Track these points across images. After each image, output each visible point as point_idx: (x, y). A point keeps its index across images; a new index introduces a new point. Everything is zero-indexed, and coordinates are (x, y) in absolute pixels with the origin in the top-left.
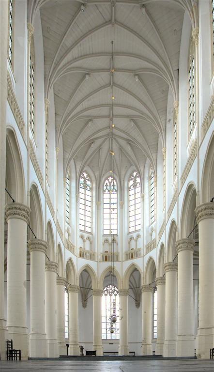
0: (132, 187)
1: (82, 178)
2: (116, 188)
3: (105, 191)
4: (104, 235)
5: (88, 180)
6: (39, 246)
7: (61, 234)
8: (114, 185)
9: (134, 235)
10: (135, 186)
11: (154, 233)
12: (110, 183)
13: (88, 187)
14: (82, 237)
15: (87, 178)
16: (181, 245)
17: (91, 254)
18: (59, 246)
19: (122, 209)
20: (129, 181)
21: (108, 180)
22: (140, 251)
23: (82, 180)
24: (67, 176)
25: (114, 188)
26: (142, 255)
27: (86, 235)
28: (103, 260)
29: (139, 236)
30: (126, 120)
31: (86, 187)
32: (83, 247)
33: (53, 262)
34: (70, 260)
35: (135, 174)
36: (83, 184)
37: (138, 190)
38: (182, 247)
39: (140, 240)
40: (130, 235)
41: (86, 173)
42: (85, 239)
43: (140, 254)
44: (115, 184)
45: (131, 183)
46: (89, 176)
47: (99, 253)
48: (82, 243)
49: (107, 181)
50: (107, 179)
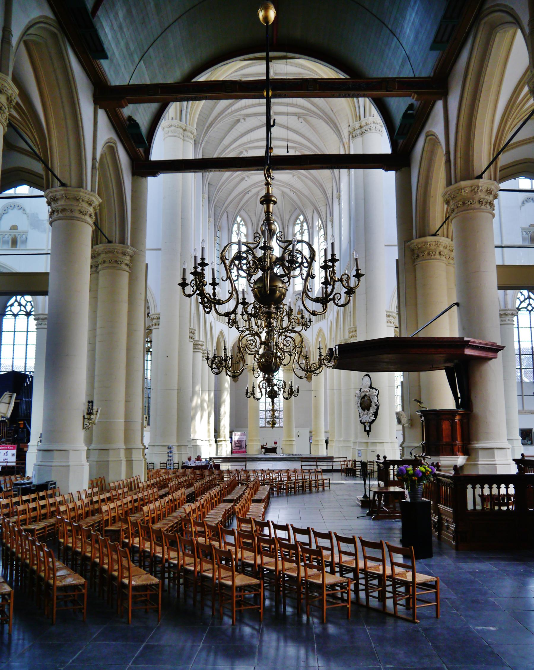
0: (298, 233)
5: (243, 225)
10: (302, 233)
20: (294, 224)
34: (221, 333)
35: (301, 218)
45: (297, 228)
46: (243, 219)
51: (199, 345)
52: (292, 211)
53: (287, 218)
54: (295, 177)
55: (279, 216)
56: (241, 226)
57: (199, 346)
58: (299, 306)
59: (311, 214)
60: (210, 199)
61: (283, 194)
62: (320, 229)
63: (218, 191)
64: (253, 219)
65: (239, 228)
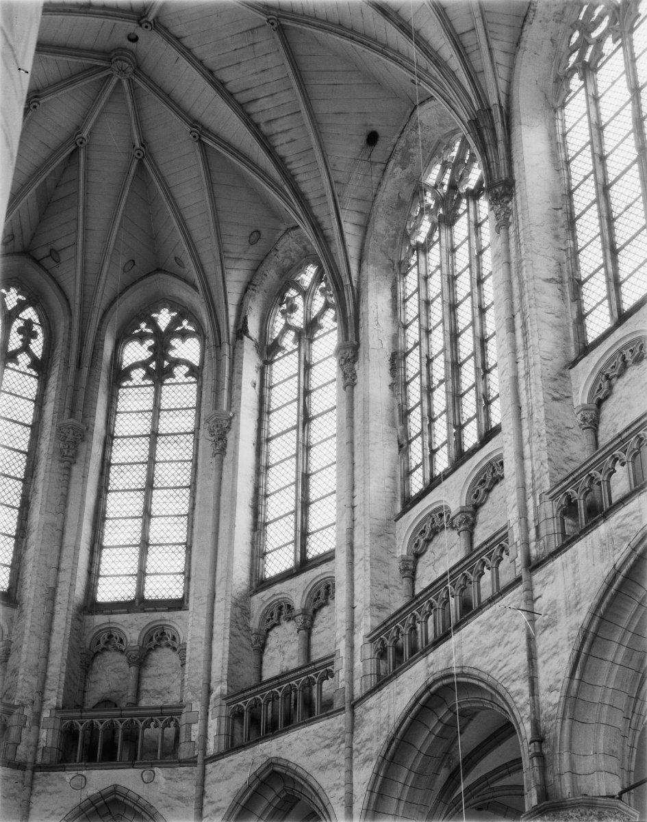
2: (37, 346)
9: (132, 628)
10: (159, 372)
20: (123, 337)
25: (25, 348)
29: (158, 638)
37: (181, 392)
40: (100, 619)
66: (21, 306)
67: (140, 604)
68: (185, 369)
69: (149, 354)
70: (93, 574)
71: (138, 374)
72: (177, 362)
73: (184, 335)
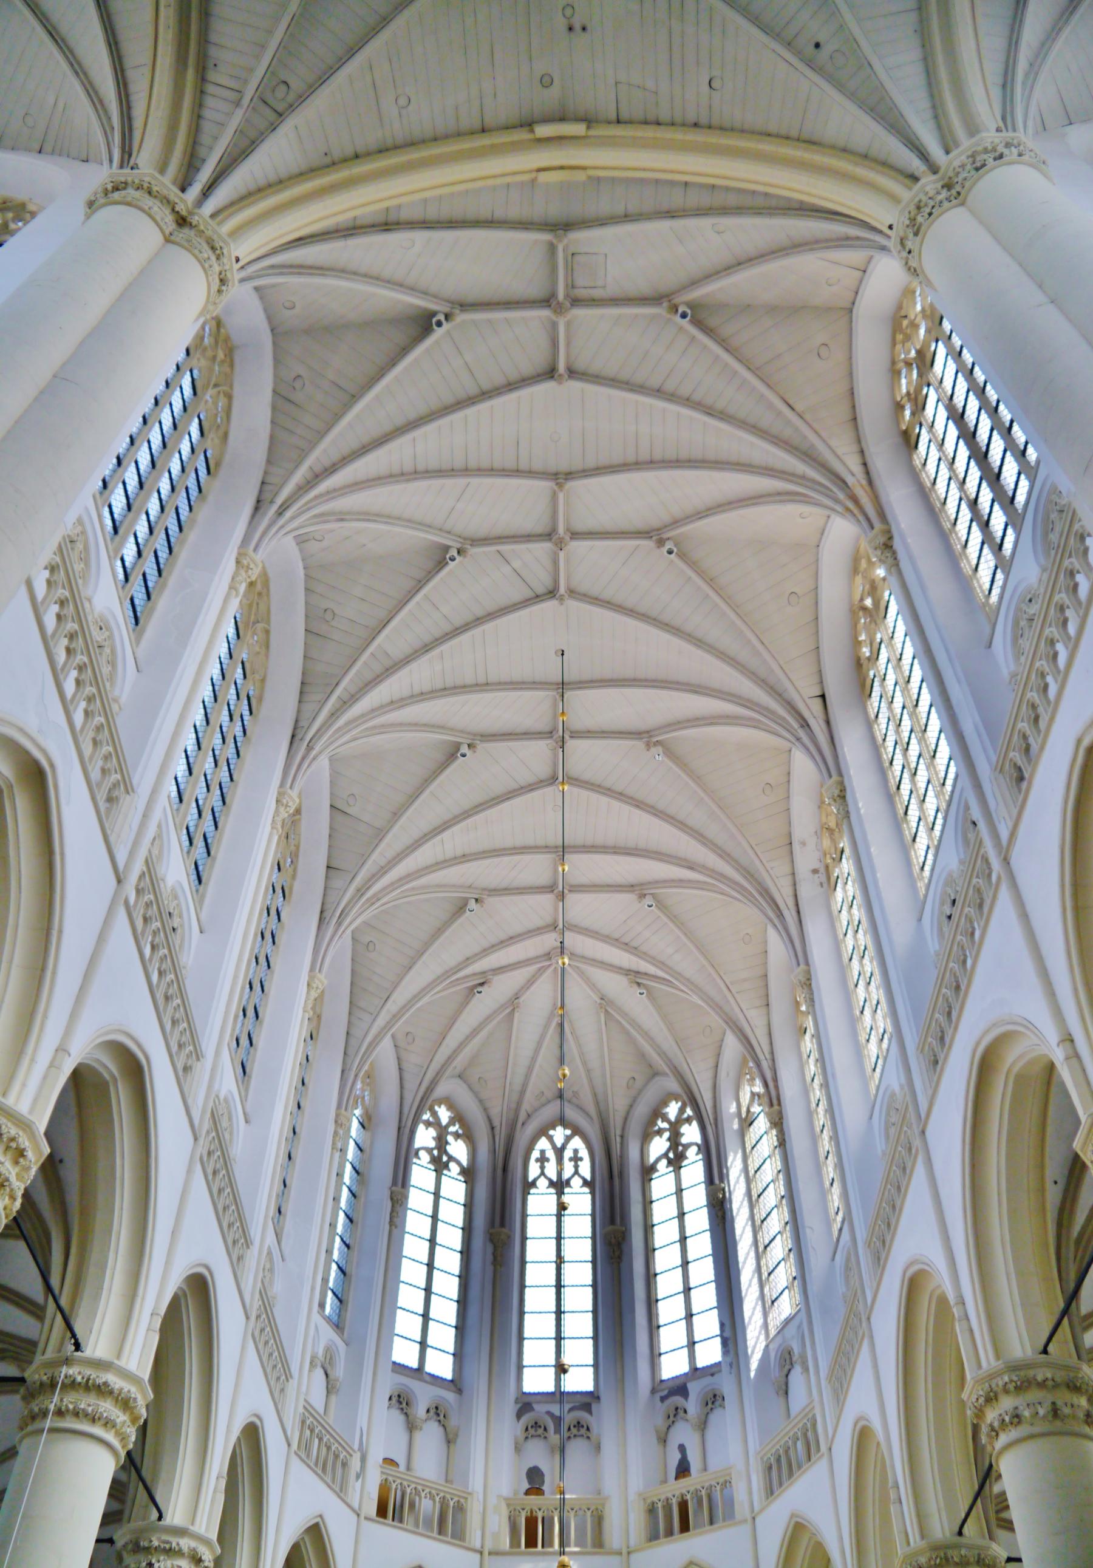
0: (664, 1162)
1: (428, 1124)
3: (533, 1184)
4: (526, 1404)
5: (457, 1136)
6: (86, 1402)
7: (277, 1370)
8: (576, 1159)
10: (676, 1160)
11: (797, 1377)
12: (559, 1152)
13: (452, 1165)
14: (401, 1401)
15: (452, 1129)
16: (1007, 1403)
17: (444, 1503)
18: (252, 1434)
19: (620, 1257)
20: (647, 1136)
21: (550, 1139)
22: (727, 1484)
23: (424, 1137)
24: (357, 1112)
25: (576, 1172)
26: (742, 1508)
27: (423, 1397)
28: (514, 1543)
30: (627, 899)
31: (446, 1166)
32: (402, 1461)
33: (181, 1532)
34: (315, 1532)
35: (672, 1110)
36: (429, 1151)
37: (694, 1170)
38: (1017, 1418)
39: (726, 1420)
41: (451, 1107)
42: (420, 1411)
43: (730, 1503)
44: (584, 1153)
45: (659, 1146)
46: (458, 1117)
47: (492, 1501)
48: (402, 1437)
49: (543, 1144)
50: (543, 1132)
51: (103, 1390)
52: (639, 1083)
53: (618, 1104)
54: (649, 900)
55: (592, 1111)
56: (450, 1138)
57: (107, 1407)
58: (682, 1448)
59: (709, 1074)
60: (327, 914)
61: (606, 1004)
62: (748, 1122)
63: (360, 892)
64: (495, 1112)
65: (441, 1143)
66: (568, 1139)
67: (695, 1371)
68: (694, 1149)
69: (668, 1144)
70: (655, 1355)
71: (662, 1165)
72: (687, 1146)
73: (688, 1120)
